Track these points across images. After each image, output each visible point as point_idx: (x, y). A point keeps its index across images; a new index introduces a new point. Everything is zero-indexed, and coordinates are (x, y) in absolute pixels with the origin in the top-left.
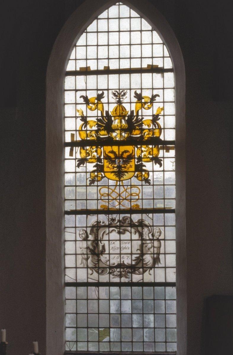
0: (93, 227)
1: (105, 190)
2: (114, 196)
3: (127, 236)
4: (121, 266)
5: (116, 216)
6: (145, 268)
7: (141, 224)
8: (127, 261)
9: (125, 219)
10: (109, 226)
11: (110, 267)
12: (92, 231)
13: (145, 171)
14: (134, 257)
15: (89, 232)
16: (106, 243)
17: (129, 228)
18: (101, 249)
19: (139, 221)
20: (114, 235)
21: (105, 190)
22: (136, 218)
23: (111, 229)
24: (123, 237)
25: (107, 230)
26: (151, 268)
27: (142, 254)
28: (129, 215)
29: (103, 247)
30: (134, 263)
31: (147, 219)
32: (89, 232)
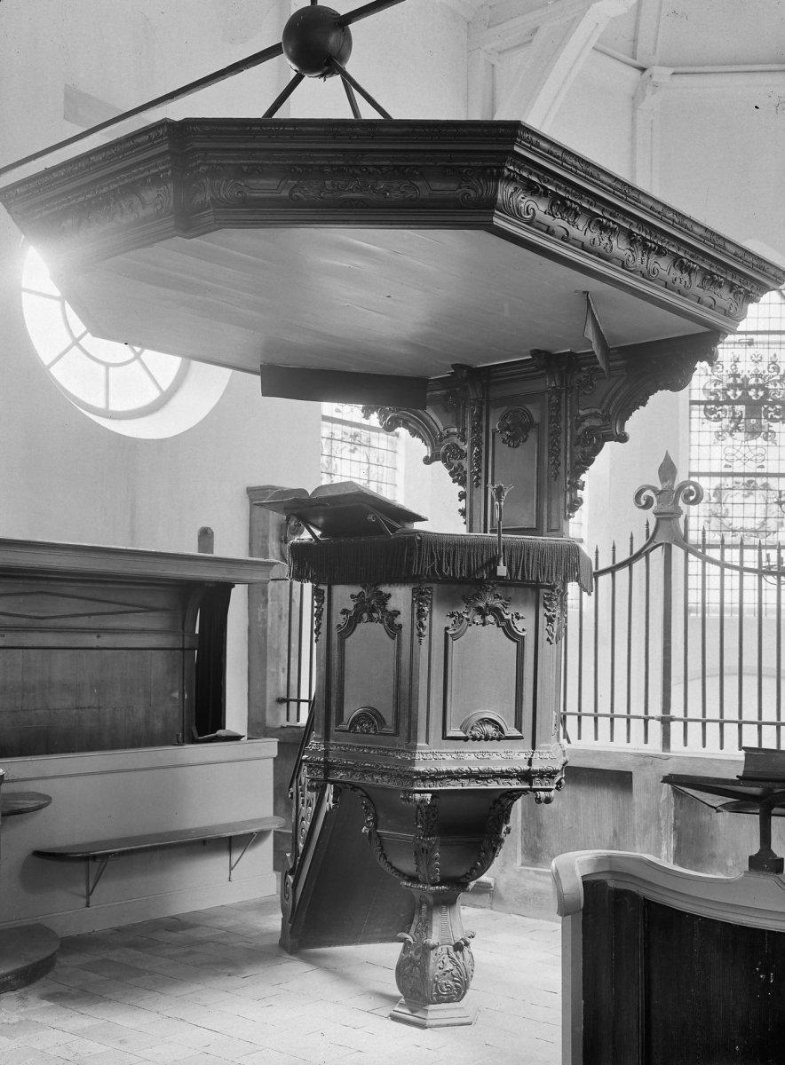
0: (716, 489)
1: (730, 451)
2: (740, 456)
3: (751, 499)
4: (743, 530)
5: (740, 479)
6: (768, 533)
7: (766, 487)
8: (750, 524)
9: (750, 482)
10: (732, 489)
11: (733, 531)
12: (715, 495)
13: (772, 432)
14: (758, 521)
15: (712, 495)
16: (729, 507)
17: (753, 492)
18: (724, 512)
19: (763, 485)
20: (738, 498)
21: (730, 451)
22: (760, 481)
23: (735, 492)
24: (747, 501)
25: (730, 492)
26: (775, 532)
27: (766, 518)
28: (753, 479)
29: (727, 510)
30: (757, 527)
31: (772, 482)
32: (712, 495)
